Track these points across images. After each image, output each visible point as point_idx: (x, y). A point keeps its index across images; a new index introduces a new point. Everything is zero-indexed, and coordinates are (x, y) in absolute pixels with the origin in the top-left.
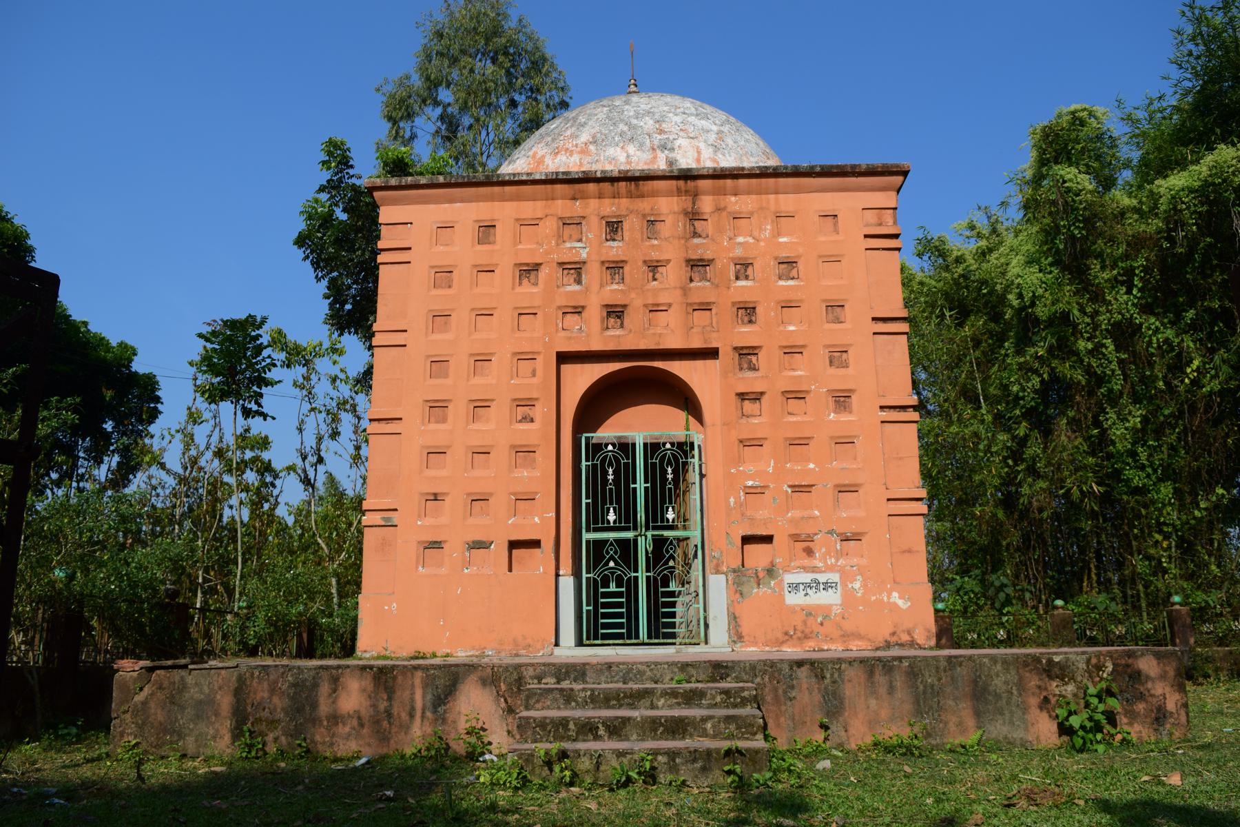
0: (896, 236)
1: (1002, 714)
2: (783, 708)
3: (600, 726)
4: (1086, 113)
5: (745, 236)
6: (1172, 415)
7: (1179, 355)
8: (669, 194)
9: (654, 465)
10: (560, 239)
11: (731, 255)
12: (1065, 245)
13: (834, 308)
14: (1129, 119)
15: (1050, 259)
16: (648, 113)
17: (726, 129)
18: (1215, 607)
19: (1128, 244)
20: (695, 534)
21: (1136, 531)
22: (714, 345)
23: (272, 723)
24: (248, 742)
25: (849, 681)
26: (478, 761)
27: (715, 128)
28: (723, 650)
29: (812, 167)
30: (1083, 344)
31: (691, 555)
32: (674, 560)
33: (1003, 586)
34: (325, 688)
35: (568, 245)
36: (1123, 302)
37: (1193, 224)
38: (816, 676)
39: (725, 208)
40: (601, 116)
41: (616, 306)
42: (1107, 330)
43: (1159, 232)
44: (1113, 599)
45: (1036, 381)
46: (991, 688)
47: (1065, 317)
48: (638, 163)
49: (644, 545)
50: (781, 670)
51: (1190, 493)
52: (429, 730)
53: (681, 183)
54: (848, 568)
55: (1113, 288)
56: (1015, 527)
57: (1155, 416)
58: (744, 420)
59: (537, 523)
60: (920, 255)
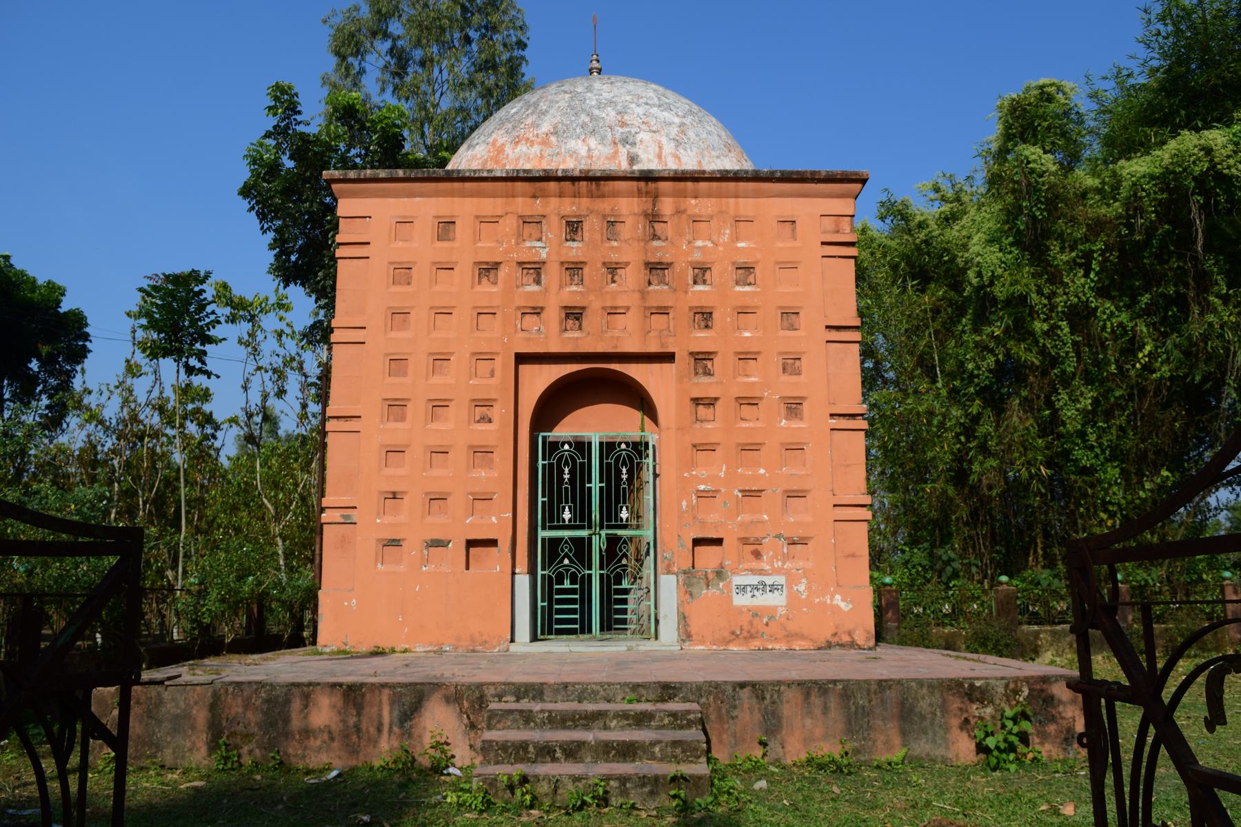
1: (925, 733)
2: (726, 726)
3: (557, 749)
4: (1054, 88)
5: (704, 240)
6: (1122, 396)
7: (1132, 340)
8: (630, 195)
9: (609, 465)
10: (521, 238)
11: (690, 259)
12: (1027, 227)
13: (789, 315)
14: (1094, 96)
15: (1011, 239)
16: (611, 102)
17: (688, 120)
18: (1155, 585)
19: (1088, 225)
20: (648, 534)
21: (1082, 510)
22: (671, 350)
23: (247, 737)
24: (224, 754)
25: (788, 702)
26: (442, 774)
27: (677, 120)
28: (672, 648)
29: (773, 173)
30: (1039, 325)
31: (643, 552)
32: (627, 558)
33: (950, 560)
34: (296, 704)
35: (528, 244)
36: (1080, 285)
37: (1153, 212)
38: (757, 697)
39: (684, 211)
40: (563, 104)
41: (575, 308)
42: (1063, 312)
43: (1119, 217)
44: (1055, 576)
45: (991, 360)
46: (917, 710)
47: (1023, 299)
48: (599, 158)
49: (598, 544)
51: (1136, 474)
52: (396, 744)
53: (642, 184)
54: (794, 571)
55: (1071, 269)
56: (965, 502)
57: (1107, 399)
58: (698, 425)
59: (495, 522)
60: (882, 219)
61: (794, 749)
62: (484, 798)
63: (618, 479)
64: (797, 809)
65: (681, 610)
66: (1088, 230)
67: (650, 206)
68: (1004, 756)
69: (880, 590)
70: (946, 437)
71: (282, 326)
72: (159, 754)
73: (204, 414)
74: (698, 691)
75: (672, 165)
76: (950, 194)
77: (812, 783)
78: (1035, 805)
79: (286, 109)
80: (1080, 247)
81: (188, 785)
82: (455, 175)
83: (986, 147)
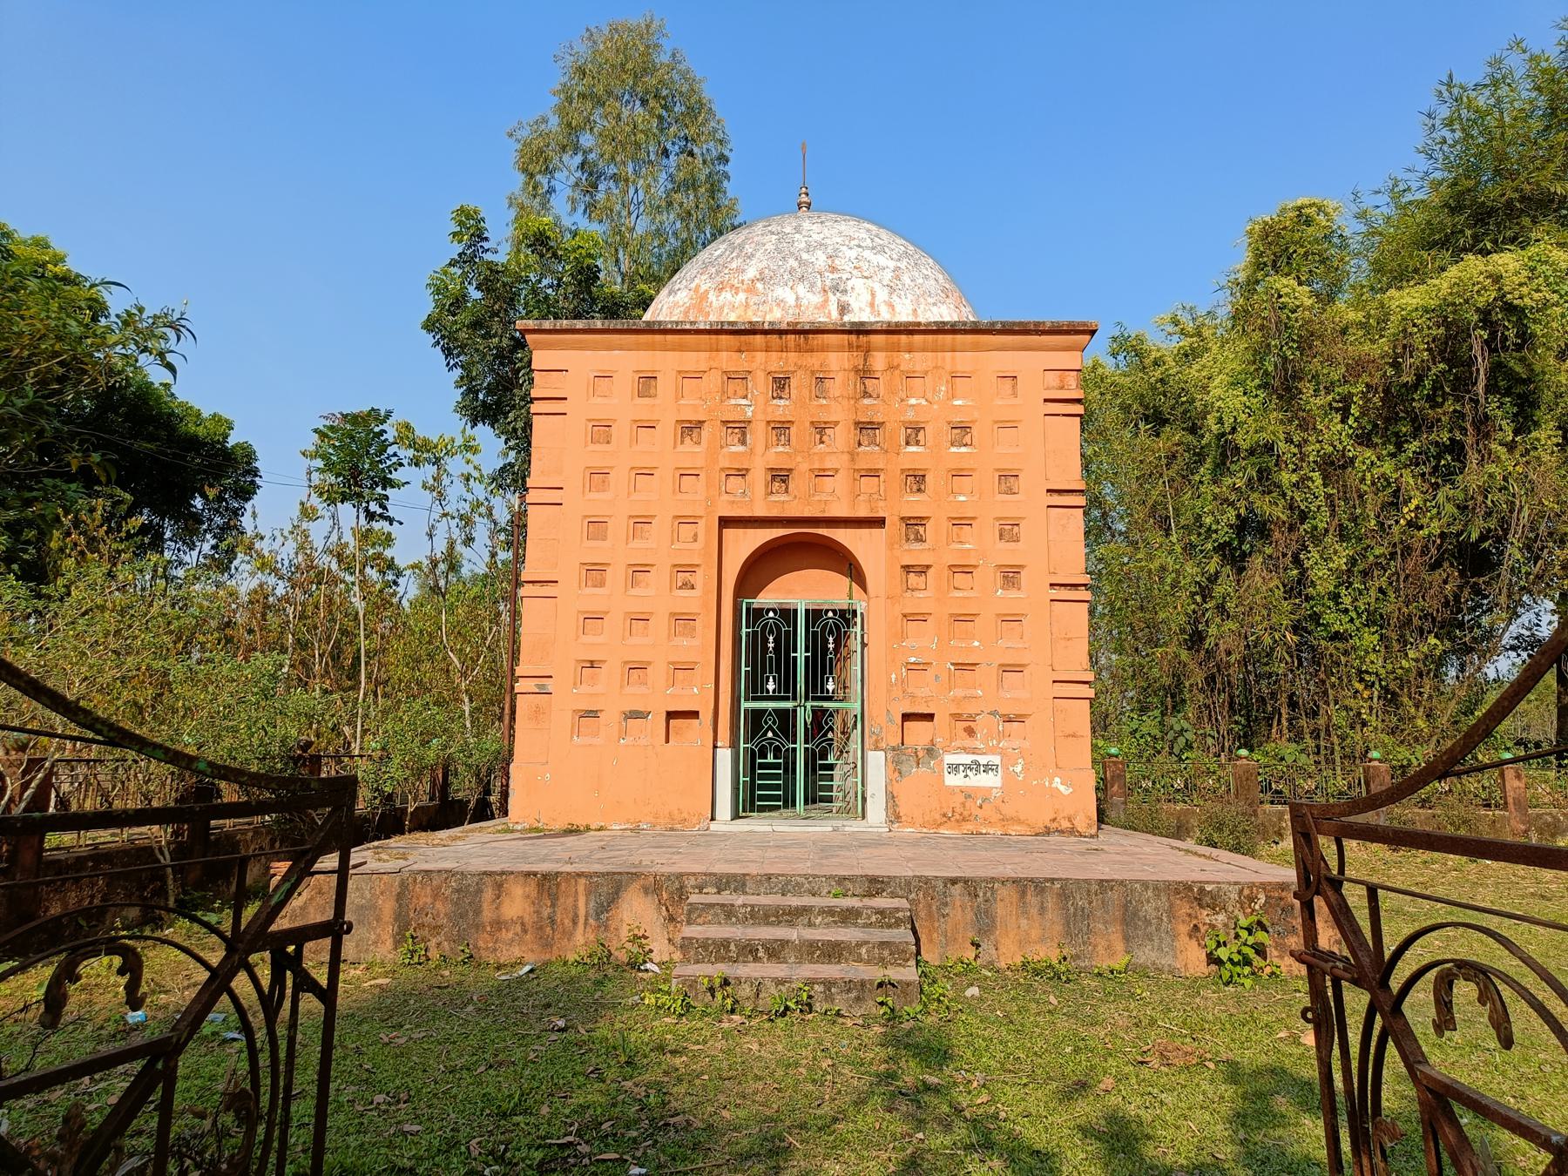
5: (918, 398)
8: (840, 349)
9: (815, 633)
13: (1007, 478)
17: (903, 265)
20: (855, 707)
22: (881, 514)
23: (436, 929)
26: (639, 970)
27: (892, 264)
29: (993, 324)
30: (1287, 476)
31: (850, 725)
34: (488, 894)
35: (733, 402)
36: (1335, 433)
40: (770, 247)
45: (1231, 514)
46: (1141, 914)
47: (1269, 448)
49: (803, 717)
53: (853, 337)
55: (1326, 414)
58: (909, 594)
59: (696, 694)
60: (1114, 355)
61: (1008, 951)
63: (825, 649)
64: (1011, 1022)
66: (1347, 371)
68: (1238, 969)
69: (1101, 761)
71: (470, 469)
73: (384, 560)
74: (908, 886)
75: (885, 316)
76: (1190, 327)
77: (1027, 991)
80: (1337, 390)
81: (372, 982)
82: (656, 327)
83: (1233, 276)
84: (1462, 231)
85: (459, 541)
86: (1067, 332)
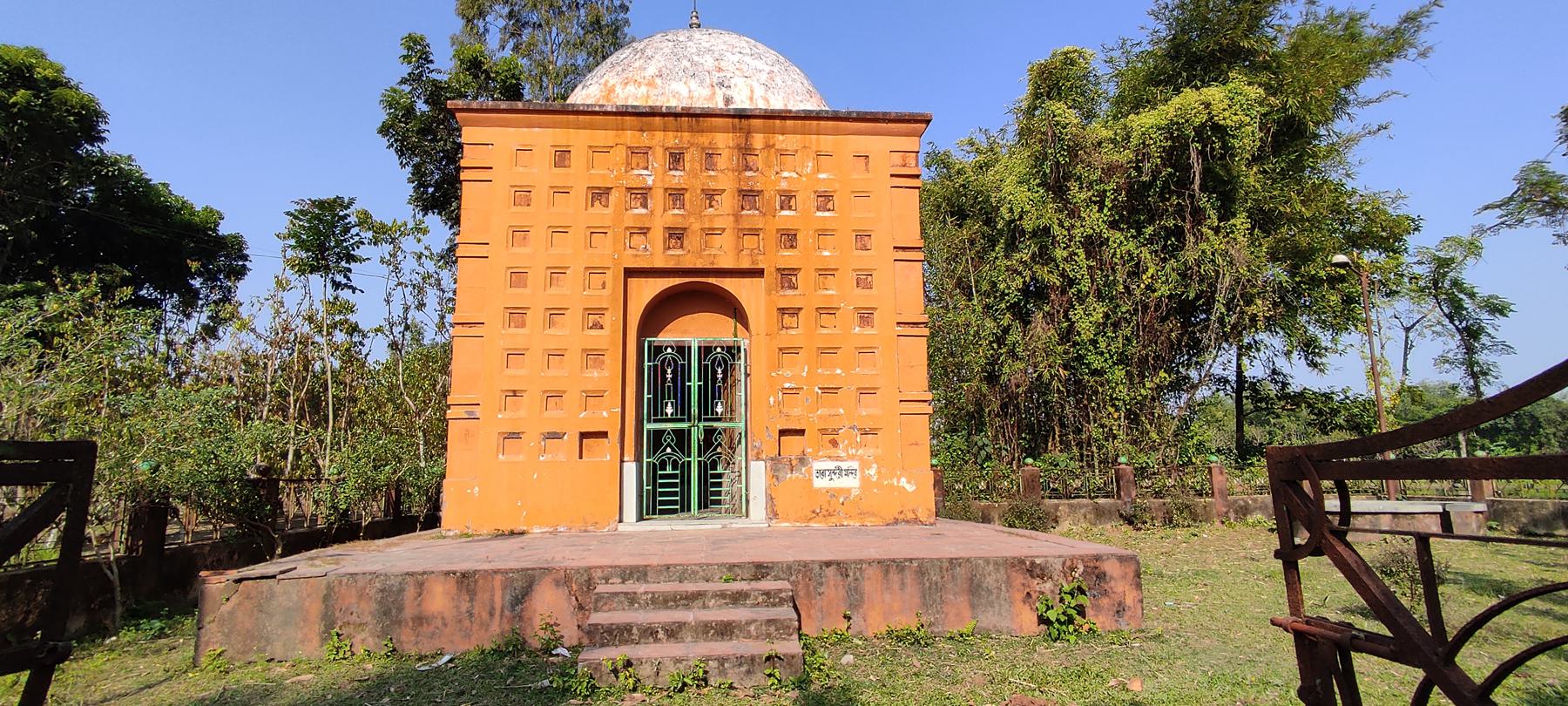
0: (917, 176)
1: (993, 607)
3: (660, 630)
6: (1128, 311)
7: (1137, 265)
9: (706, 366)
10: (629, 166)
12: (1051, 170)
17: (776, 69)
25: (868, 579)
27: (767, 69)
28: (761, 525)
29: (850, 113)
34: (410, 592)
35: (636, 172)
36: (1094, 220)
40: (667, 51)
45: (1019, 281)
46: (984, 585)
47: (1047, 230)
49: (696, 436)
50: (812, 569)
52: (507, 627)
53: (736, 121)
55: (1088, 206)
58: (784, 331)
60: (928, 166)
62: (588, 683)
63: (715, 379)
65: (769, 492)
67: (744, 142)
68: (1064, 627)
70: (981, 345)
71: (420, 248)
72: (269, 648)
74: (789, 570)
75: (762, 105)
76: (984, 146)
78: (1104, 681)
79: (420, 57)
81: (294, 679)
82: (570, 109)
83: (1017, 104)
84: (1180, 73)
85: (413, 306)
86: (908, 121)
